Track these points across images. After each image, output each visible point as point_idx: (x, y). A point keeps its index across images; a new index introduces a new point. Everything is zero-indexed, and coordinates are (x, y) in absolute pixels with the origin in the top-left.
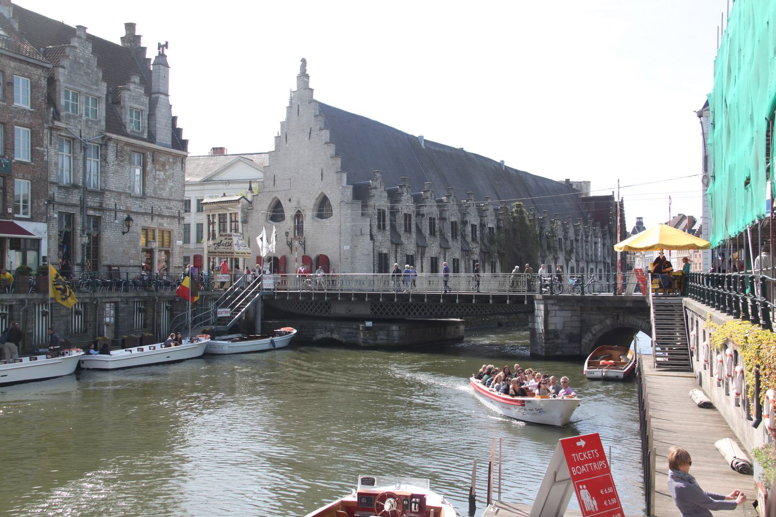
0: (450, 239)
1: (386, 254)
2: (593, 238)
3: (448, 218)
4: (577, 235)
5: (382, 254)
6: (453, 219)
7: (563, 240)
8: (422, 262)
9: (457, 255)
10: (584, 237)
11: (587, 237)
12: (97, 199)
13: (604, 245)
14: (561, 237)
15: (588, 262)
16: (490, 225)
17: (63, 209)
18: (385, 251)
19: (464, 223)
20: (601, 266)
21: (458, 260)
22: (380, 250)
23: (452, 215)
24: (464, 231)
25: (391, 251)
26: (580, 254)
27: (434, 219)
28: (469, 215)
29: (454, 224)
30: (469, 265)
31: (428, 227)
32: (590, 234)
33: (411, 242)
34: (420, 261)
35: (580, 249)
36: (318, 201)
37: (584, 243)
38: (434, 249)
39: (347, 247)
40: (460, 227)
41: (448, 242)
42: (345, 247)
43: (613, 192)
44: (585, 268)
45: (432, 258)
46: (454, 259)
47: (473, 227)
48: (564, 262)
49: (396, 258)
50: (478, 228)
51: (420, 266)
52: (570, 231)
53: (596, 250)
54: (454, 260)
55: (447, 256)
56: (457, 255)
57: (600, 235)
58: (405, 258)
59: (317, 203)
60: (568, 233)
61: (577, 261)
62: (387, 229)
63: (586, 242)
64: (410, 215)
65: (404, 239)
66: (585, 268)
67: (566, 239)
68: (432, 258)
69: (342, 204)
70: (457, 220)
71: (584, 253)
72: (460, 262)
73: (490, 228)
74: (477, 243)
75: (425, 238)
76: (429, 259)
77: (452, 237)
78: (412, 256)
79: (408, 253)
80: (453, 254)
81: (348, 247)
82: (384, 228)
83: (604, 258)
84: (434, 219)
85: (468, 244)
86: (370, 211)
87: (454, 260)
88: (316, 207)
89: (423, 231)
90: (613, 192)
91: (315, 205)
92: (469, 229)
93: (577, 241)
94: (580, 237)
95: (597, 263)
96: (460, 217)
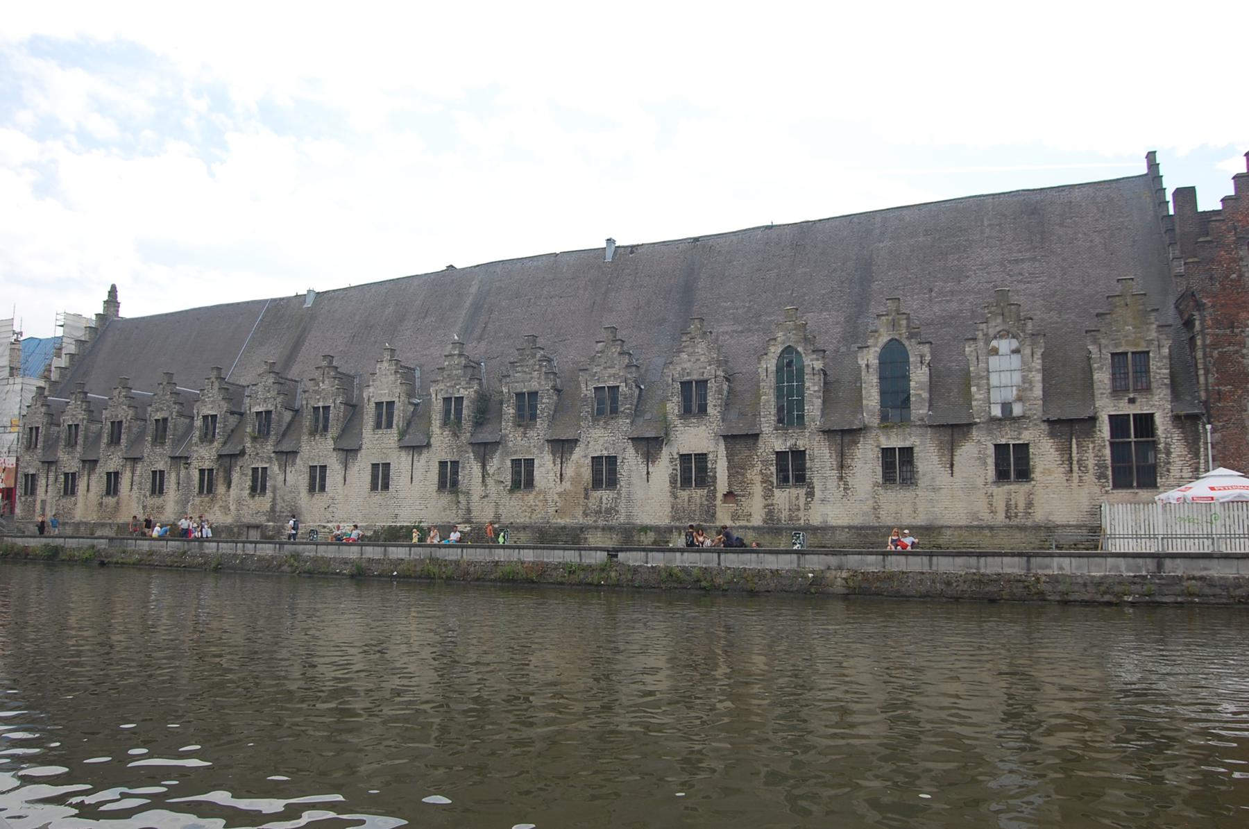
6: (159, 416)
18: (32, 471)
21: (162, 472)
22: (26, 470)
33: (73, 457)
34: (86, 478)
45: (109, 474)
46: (154, 473)
51: (86, 485)
54: (154, 473)
58: (62, 476)
68: (109, 474)
72: (166, 475)
73: (258, 413)
78: (74, 474)
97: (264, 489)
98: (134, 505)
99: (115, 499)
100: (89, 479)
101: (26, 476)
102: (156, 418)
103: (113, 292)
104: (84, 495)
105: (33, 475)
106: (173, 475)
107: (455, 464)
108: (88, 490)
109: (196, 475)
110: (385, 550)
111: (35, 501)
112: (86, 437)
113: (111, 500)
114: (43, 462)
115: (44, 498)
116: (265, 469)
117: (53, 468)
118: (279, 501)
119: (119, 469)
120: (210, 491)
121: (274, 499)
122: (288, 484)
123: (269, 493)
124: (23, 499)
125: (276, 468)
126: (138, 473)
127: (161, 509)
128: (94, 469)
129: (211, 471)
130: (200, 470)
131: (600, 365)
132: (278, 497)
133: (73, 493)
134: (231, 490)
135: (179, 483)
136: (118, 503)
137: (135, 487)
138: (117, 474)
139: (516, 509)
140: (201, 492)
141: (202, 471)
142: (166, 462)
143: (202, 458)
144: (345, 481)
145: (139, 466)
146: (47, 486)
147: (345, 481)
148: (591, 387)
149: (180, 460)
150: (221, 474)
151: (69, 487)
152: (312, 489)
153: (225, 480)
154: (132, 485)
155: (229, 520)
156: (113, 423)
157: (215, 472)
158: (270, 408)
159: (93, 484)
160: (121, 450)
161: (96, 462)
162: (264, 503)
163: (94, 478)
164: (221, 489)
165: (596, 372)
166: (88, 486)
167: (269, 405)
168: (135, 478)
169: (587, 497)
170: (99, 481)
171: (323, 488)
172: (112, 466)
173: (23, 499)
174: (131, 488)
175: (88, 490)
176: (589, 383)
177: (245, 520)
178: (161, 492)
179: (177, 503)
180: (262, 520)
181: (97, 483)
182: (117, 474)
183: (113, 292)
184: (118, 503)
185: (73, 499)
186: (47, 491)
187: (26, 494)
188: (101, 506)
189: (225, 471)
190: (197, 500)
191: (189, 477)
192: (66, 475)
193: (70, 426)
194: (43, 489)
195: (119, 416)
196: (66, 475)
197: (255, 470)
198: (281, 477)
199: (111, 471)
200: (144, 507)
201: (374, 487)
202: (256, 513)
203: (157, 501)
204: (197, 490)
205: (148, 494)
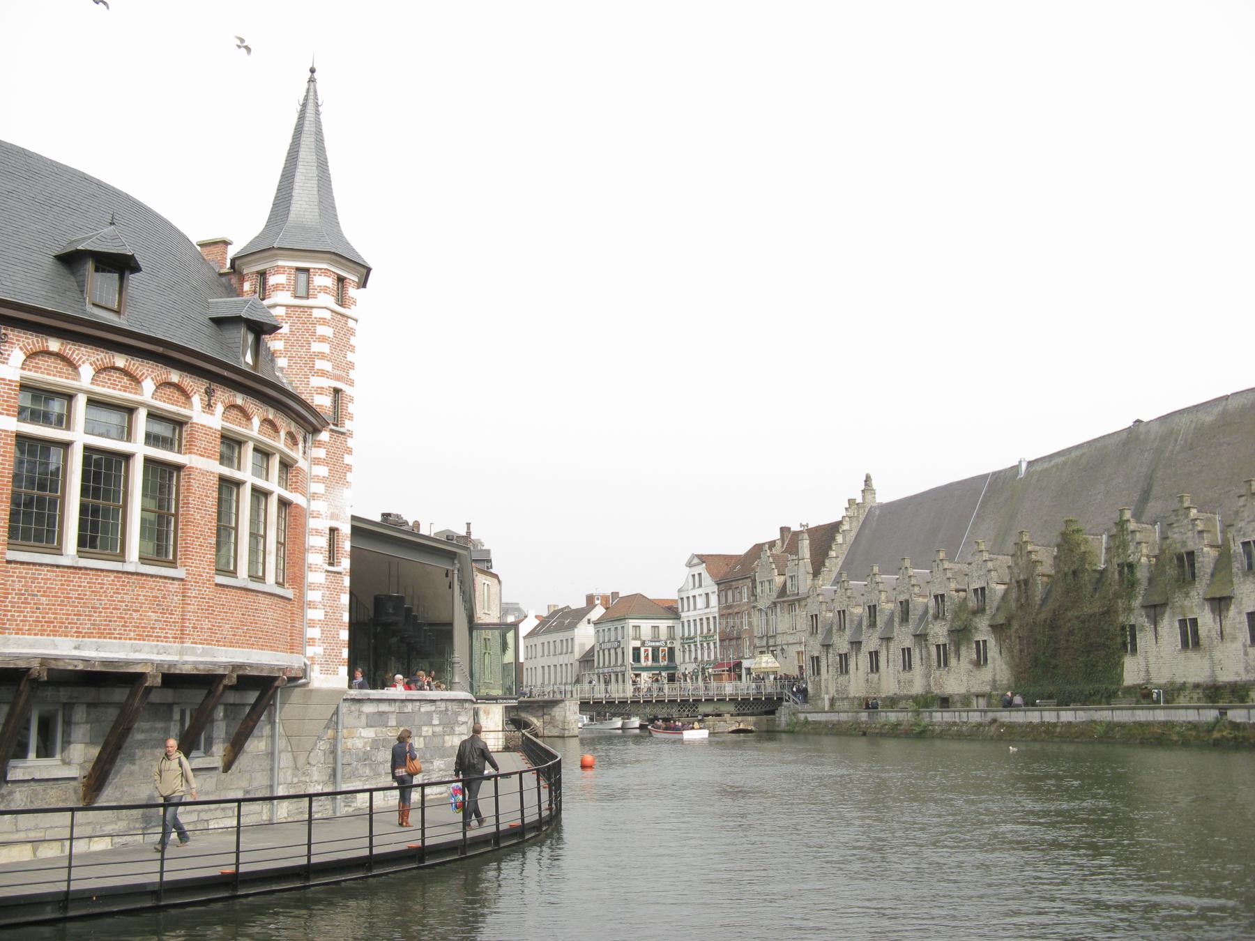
9: (908, 643)
12: (773, 640)
17: (760, 650)
18: (815, 655)
21: (909, 649)
30: (929, 655)
34: (855, 658)
38: (871, 642)
45: (871, 653)
46: (903, 650)
54: (903, 650)
56: (908, 643)
58: (838, 657)
68: (871, 653)
78: (846, 655)
79: (841, 652)
97: (986, 660)
99: (877, 676)
101: (813, 658)
103: (868, 480)
105: (817, 657)
106: (917, 651)
108: (857, 669)
109: (933, 650)
110: (1058, 714)
111: (820, 680)
112: (852, 621)
113: (874, 677)
114: (823, 646)
116: (985, 642)
117: (831, 651)
119: (878, 647)
120: (946, 664)
121: (994, 669)
125: (993, 642)
126: (891, 651)
127: (911, 682)
128: (859, 649)
129: (945, 645)
131: (1244, 520)
133: (847, 672)
134: (961, 662)
136: (879, 679)
138: (876, 653)
139: (1194, 669)
140: (939, 665)
141: (938, 647)
143: (937, 634)
145: (892, 645)
148: (1239, 543)
149: (921, 637)
150: (953, 648)
151: (843, 664)
153: (956, 654)
155: (963, 691)
156: (869, 607)
158: (983, 584)
163: (861, 656)
164: (953, 661)
165: (1241, 528)
168: (890, 656)
169: (1246, 654)
173: (812, 679)
175: (857, 669)
176: (1236, 539)
177: (973, 690)
180: (987, 689)
181: (864, 661)
182: (876, 653)
183: (868, 480)
184: (879, 679)
187: (814, 674)
189: (955, 646)
190: (938, 672)
192: (840, 655)
193: (839, 612)
196: (840, 655)
199: (872, 650)
200: (899, 682)
203: (907, 675)
204: (936, 664)
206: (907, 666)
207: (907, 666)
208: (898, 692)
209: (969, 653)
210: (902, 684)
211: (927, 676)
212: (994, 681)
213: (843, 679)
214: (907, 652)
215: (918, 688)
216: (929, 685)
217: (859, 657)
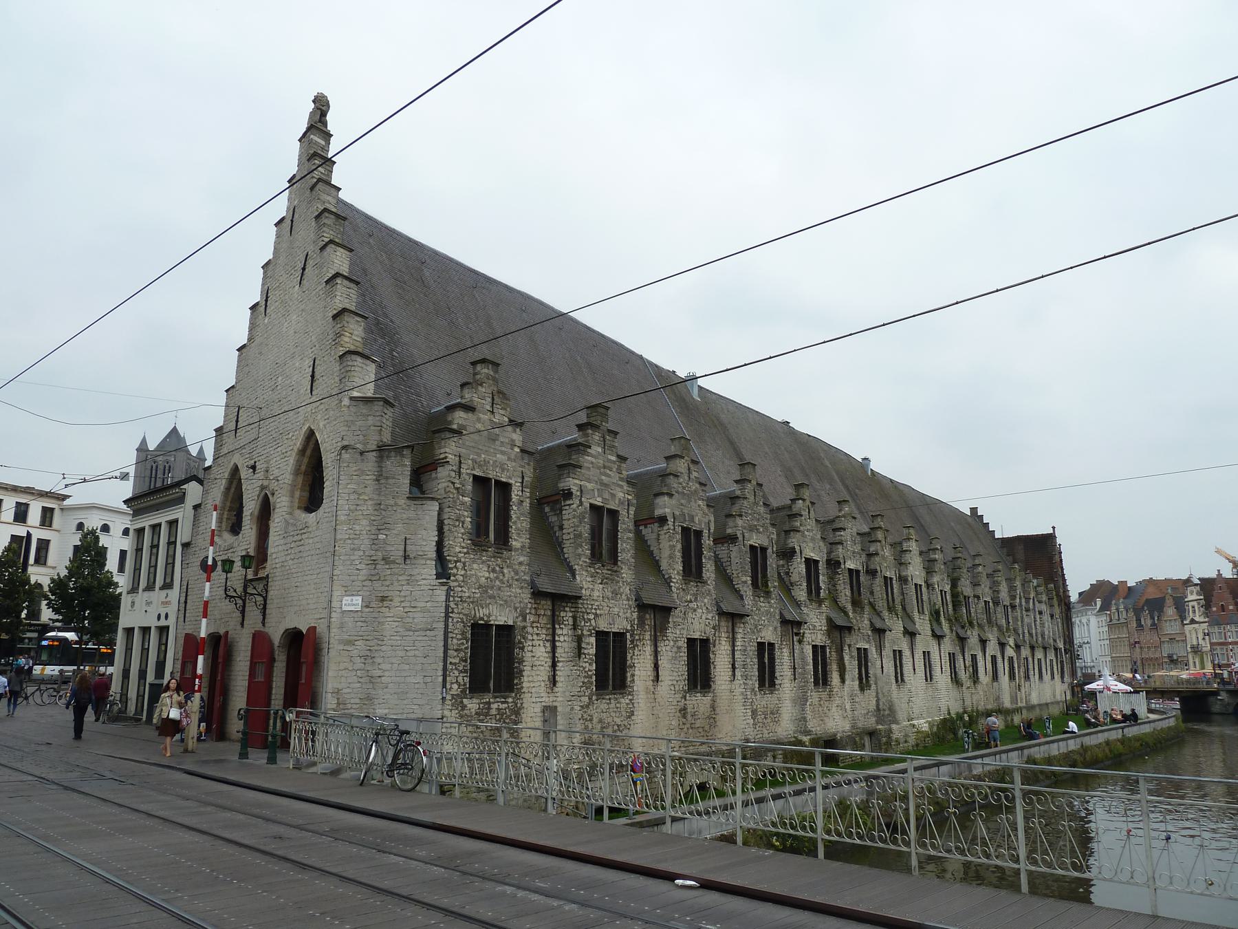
0: (747, 591)
1: (506, 631)
2: (1036, 603)
3: (741, 538)
4: (1013, 597)
5: (488, 626)
6: (755, 540)
7: (991, 604)
8: (656, 653)
9: (769, 634)
10: (1023, 600)
11: (1027, 600)
13: (1052, 616)
14: (988, 599)
15: (1032, 648)
16: (851, 565)
18: (501, 616)
19: (788, 554)
20: (1053, 658)
21: (771, 645)
22: (482, 613)
23: (752, 529)
24: (787, 573)
25: (530, 618)
26: (1020, 632)
27: (699, 534)
28: (798, 535)
29: (758, 554)
31: (679, 555)
32: (1032, 596)
33: (616, 593)
34: (649, 649)
35: (1019, 623)
36: (306, 460)
37: (1024, 612)
39: (353, 603)
40: (772, 561)
41: (741, 597)
42: (347, 600)
43: (1054, 528)
44: (1030, 659)
45: (691, 642)
47: (811, 564)
48: (998, 647)
49: (553, 642)
50: (822, 566)
51: (649, 665)
52: (1001, 588)
53: (1042, 625)
54: (761, 646)
55: (739, 636)
57: (1044, 598)
58: (593, 640)
59: (303, 468)
60: (998, 592)
61: (1018, 647)
62: (515, 544)
63: (1027, 610)
64: (614, 514)
65: (587, 582)
66: (1030, 659)
67: (996, 603)
68: (691, 642)
69: (346, 456)
70: (765, 543)
71: (1026, 631)
72: (777, 653)
74: (820, 602)
75: (667, 582)
76: (683, 644)
77: (755, 584)
78: (620, 636)
79: (603, 626)
80: (757, 629)
81: (358, 600)
82: (503, 539)
83: (1055, 641)
84: (699, 534)
85: (798, 605)
86: (442, 479)
87: (761, 646)
88: (300, 479)
89: (664, 565)
90: (1054, 528)
91: (297, 472)
92: (798, 569)
93: (1013, 607)
94: (1018, 600)
95: (1045, 648)
96: (774, 537)
98: (739, 709)
99: (707, 699)
100: (656, 653)
102: (751, 542)
104: (647, 691)
106: (786, 652)
107: (953, 654)
108: (657, 678)
111: (517, 711)
113: (699, 702)
115: (547, 700)
117: (567, 615)
118: (880, 696)
119: (710, 632)
121: (877, 693)
122: (885, 671)
123: (873, 687)
124: (472, 705)
125: (874, 650)
126: (739, 642)
127: (775, 713)
130: (813, 646)
132: (879, 691)
135: (795, 668)
136: (713, 708)
137: (738, 673)
138: (705, 642)
140: (816, 683)
141: (814, 647)
142: (775, 628)
144: (914, 670)
146: (554, 665)
147: (914, 670)
149: (792, 626)
152: (897, 681)
154: (734, 668)
157: (828, 650)
159: (664, 663)
160: (709, 593)
161: (666, 611)
162: (868, 701)
164: (835, 678)
166: (656, 667)
167: (858, 563)
170: (675, 658)
171: (903, 680)
172: (697, 626)
174: (734, 675)
175: (657, 678)
178: (772, 684)
179: (794, 701)
184: (713, 708)
185: (625, 701)
186: (553, 681)
188: (684, 716)
191: (803, 659)
192: (601, 636)
194: (544, 672)
195: (696, 520)
197: (859, 649)
198: (879, 663)
199: (697, 636)
200: (754, 713)
201: (926, 680)
202: (867, 714)
205: (757, 686)
206: (767, 679)
207: (767, 679)
208: (750, 733)
209: (851, 665)
210: (760, 718)
211: (801, 701)
212: (878, 709)
213: (607, 709)
214: (765, 651)
215: (785, 727)
216: (804, 719)
217: (661, 645)
